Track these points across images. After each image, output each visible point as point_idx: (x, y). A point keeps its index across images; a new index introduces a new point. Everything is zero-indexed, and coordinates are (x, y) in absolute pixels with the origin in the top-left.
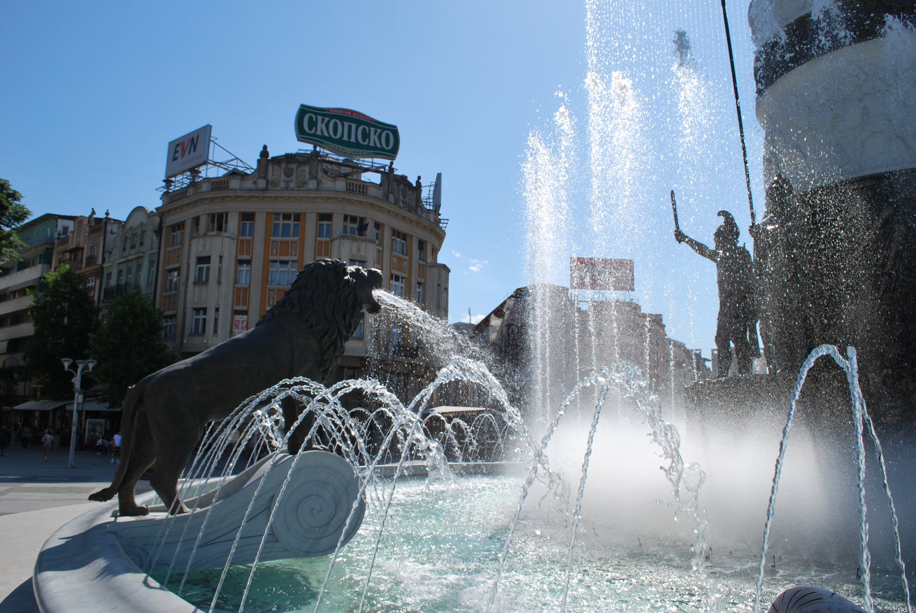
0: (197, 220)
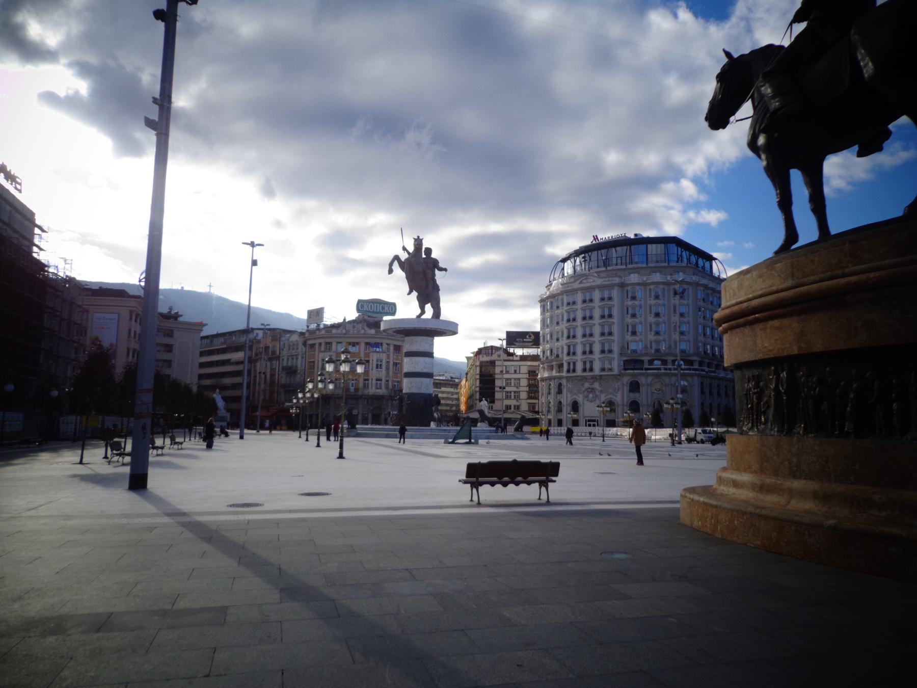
0: (320, 344)
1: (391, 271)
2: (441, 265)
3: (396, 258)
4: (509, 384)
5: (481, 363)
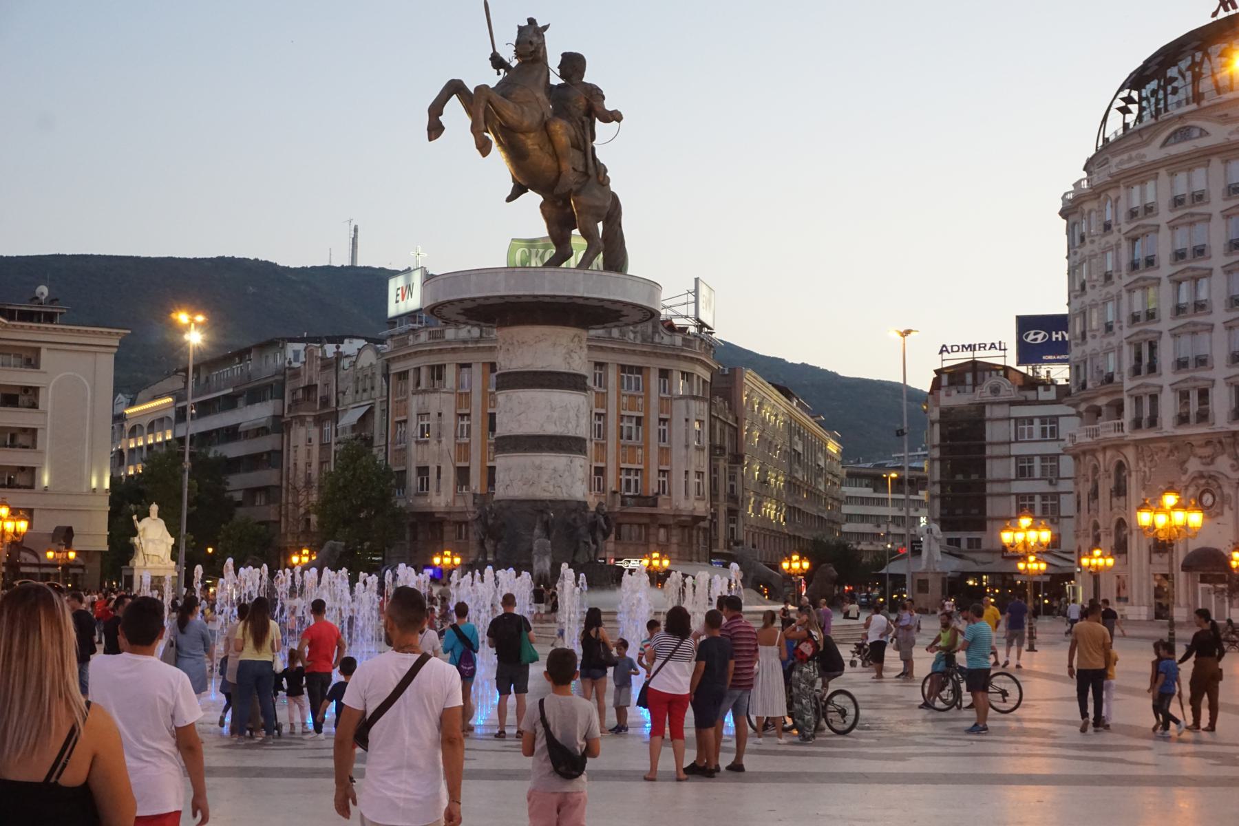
0: (419, 369)
1: (435, 129)
2: (609, 105)
3: (455, 88)
4: (1024, 473)
5: (946, 413)
